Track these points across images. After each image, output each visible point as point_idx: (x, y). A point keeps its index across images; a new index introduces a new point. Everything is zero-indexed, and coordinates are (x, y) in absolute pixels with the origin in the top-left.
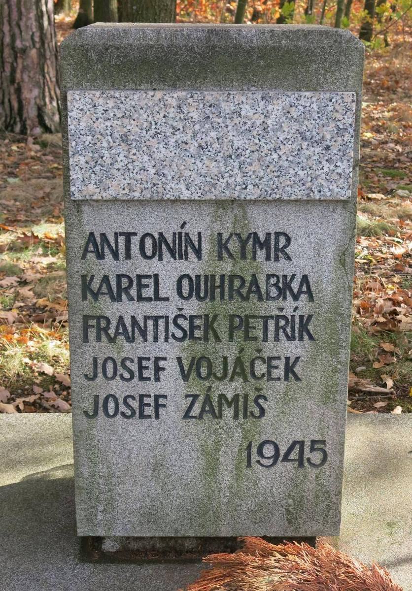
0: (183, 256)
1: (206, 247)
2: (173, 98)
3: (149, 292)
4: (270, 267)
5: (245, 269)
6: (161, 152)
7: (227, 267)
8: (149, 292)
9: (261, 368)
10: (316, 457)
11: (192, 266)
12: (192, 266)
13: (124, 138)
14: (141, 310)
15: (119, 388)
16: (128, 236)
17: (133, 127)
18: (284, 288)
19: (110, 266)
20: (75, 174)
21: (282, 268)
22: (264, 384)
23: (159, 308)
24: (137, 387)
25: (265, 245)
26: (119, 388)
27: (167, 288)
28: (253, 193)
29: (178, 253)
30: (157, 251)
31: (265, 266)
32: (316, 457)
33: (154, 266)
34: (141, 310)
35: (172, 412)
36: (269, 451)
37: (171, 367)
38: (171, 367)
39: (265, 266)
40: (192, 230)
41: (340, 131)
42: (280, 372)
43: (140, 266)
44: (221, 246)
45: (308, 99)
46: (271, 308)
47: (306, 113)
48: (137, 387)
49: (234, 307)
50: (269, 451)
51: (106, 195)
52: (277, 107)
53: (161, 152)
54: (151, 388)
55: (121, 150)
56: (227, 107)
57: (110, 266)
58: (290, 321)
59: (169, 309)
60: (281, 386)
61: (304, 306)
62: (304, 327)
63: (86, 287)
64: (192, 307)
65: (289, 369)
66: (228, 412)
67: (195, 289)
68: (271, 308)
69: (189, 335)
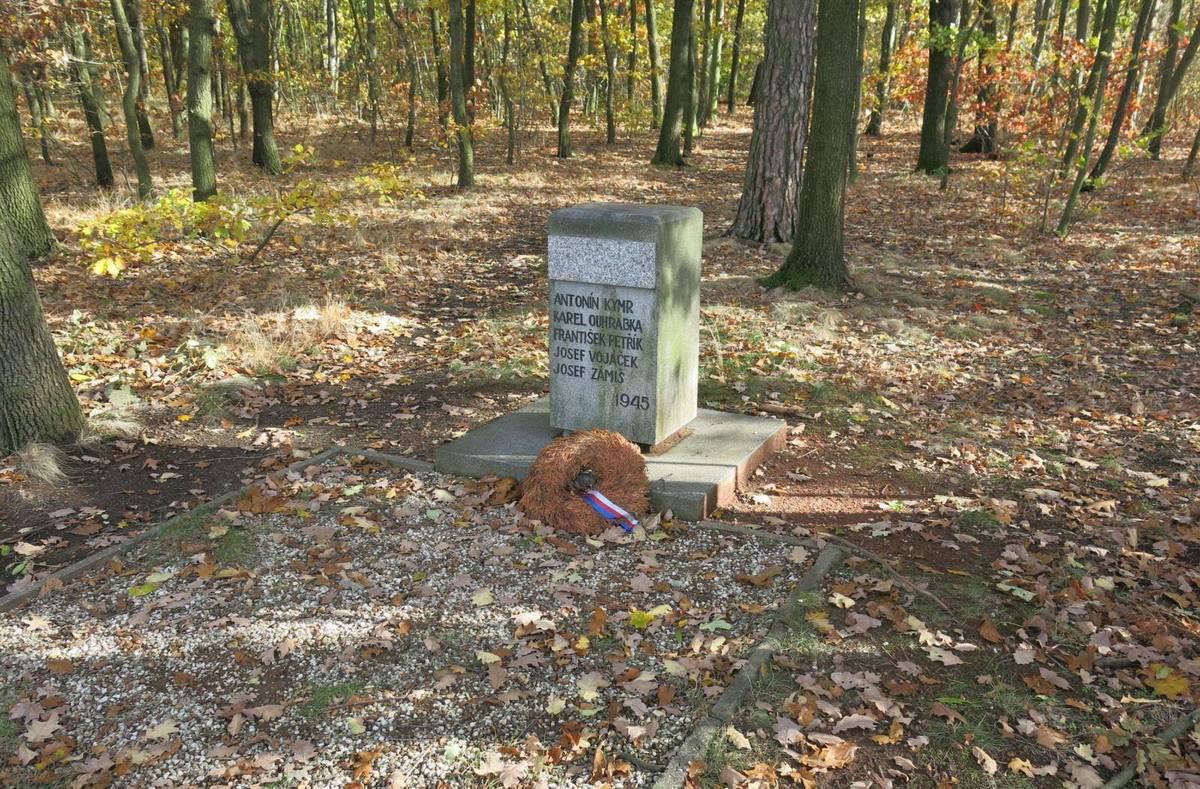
0: (592, 307)
1: (600, 304)
2: (585, 240)
3: (578, 321)
4: (624, 315)
6: (581, 262)
8: (578, 321)
9: (622, 360)
10: (644, 405)
11: (595, 312)
12: (595, 312)
13: (568, 256)
14: (576, 328)
15: (567, 362)
16: (571, 296)
17: (570, 251)
18: (631, 326)
19: (564, 308)
21: (629, 316)
24: (574, 362)
26: (567, 362)
27: (586, 320)
28: (614, 283)
30: (582, 305)
34: (576, 328)
35: (587, 375)
37: (586, 355)
38: (586, 354)
40: (595, 296)
41: (648, 259)
42: (629, 363)
43: (575, 309)
44: (606, 304)
45: (636, 245)
46: (625, 333)
47: (635, 251)
48: (574, 362)
49: (611, 331)
51: (562, 278)
52: (623, 248)
53: (581, 262)
54: (579, 363)
56: (605, 246)
57: (564, 308)
58: (633, 340)
59: (586, 329)
60: (630, 369)
62: (638, 344)
64: (595, 330)
65: (633, 362)
66: (609, 379)
67: (596, 322)
68: (625, 333)
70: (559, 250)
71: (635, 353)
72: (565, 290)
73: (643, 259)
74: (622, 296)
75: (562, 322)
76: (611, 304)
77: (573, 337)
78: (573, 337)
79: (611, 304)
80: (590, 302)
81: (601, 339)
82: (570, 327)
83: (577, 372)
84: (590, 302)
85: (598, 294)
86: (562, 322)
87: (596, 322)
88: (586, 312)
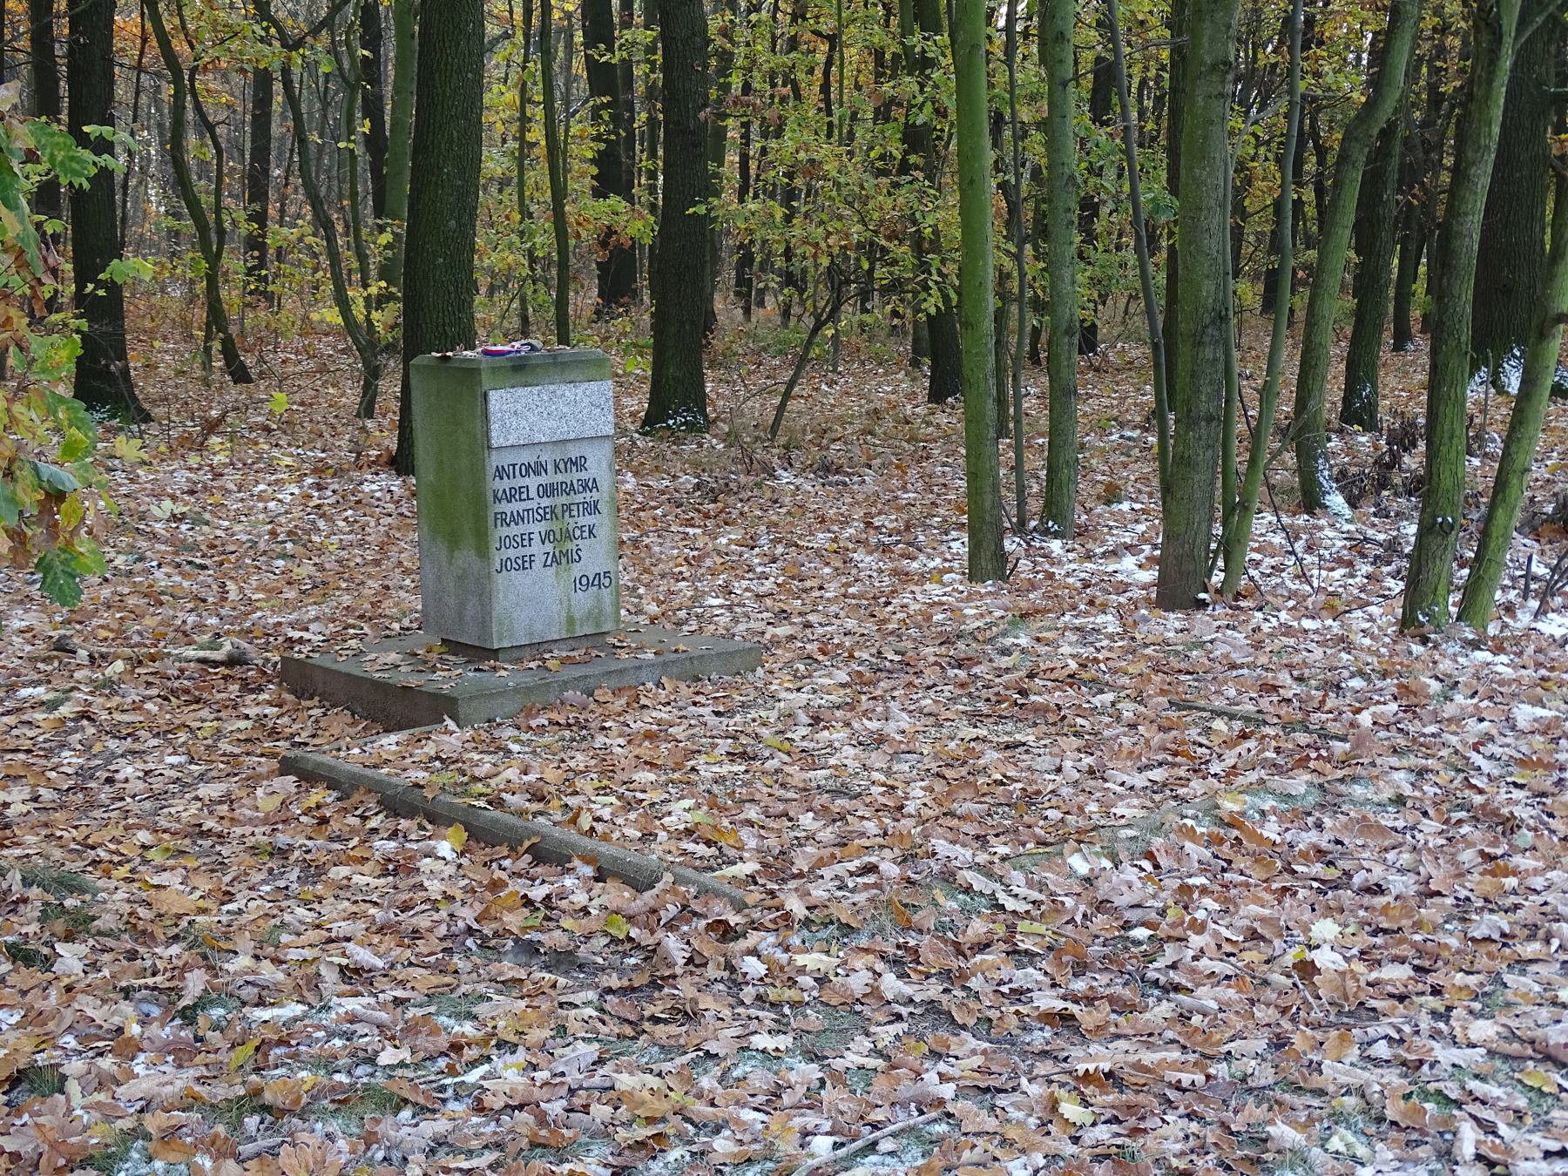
1: (550, 468)
2: (535, 390)
3: (524, 496)
7: (560, 478)
8: (524, 496)
9: (578, 533)
11: (543, 479)
12: (543, 479)
14: (524, 505)
15: (512, 553)
17: (519, 407)
18: (585, 487)
20: (494, 434)
21: (583, 475)
22: (579, 542)
24: (521, 551)
25: (575, 464)
26: (512, 553)
27: (533, 493)
29: (537, 473)
31: (574, 476)
33: (527, 481)
35: (538, 564)
39: (574, 476)
40: (542, 459)
42: (586, 534)
43: (519, 482)
46: (579, 498)
48: (521, 551)
49: (564, 499)
52: (580, 391)
54: (527, 551)
55: (514, 419)
59: (532, 505)
61: (595, 495)
64: (545, 502)
68: (579, 498)
70: (505, 407)
71: (587, 520)
72: (505, 460)
73: (602, 401)
74: (574, 452)
75: (504, 502)
76: (562, 466)
77: (518, 518)
79: (562, 466)
80: (537, 469)
81: (553, 512)
82: (516, 506)
84: (537, 469)
86: (504, 502)
87: (545, 491)
88: (533, 482)
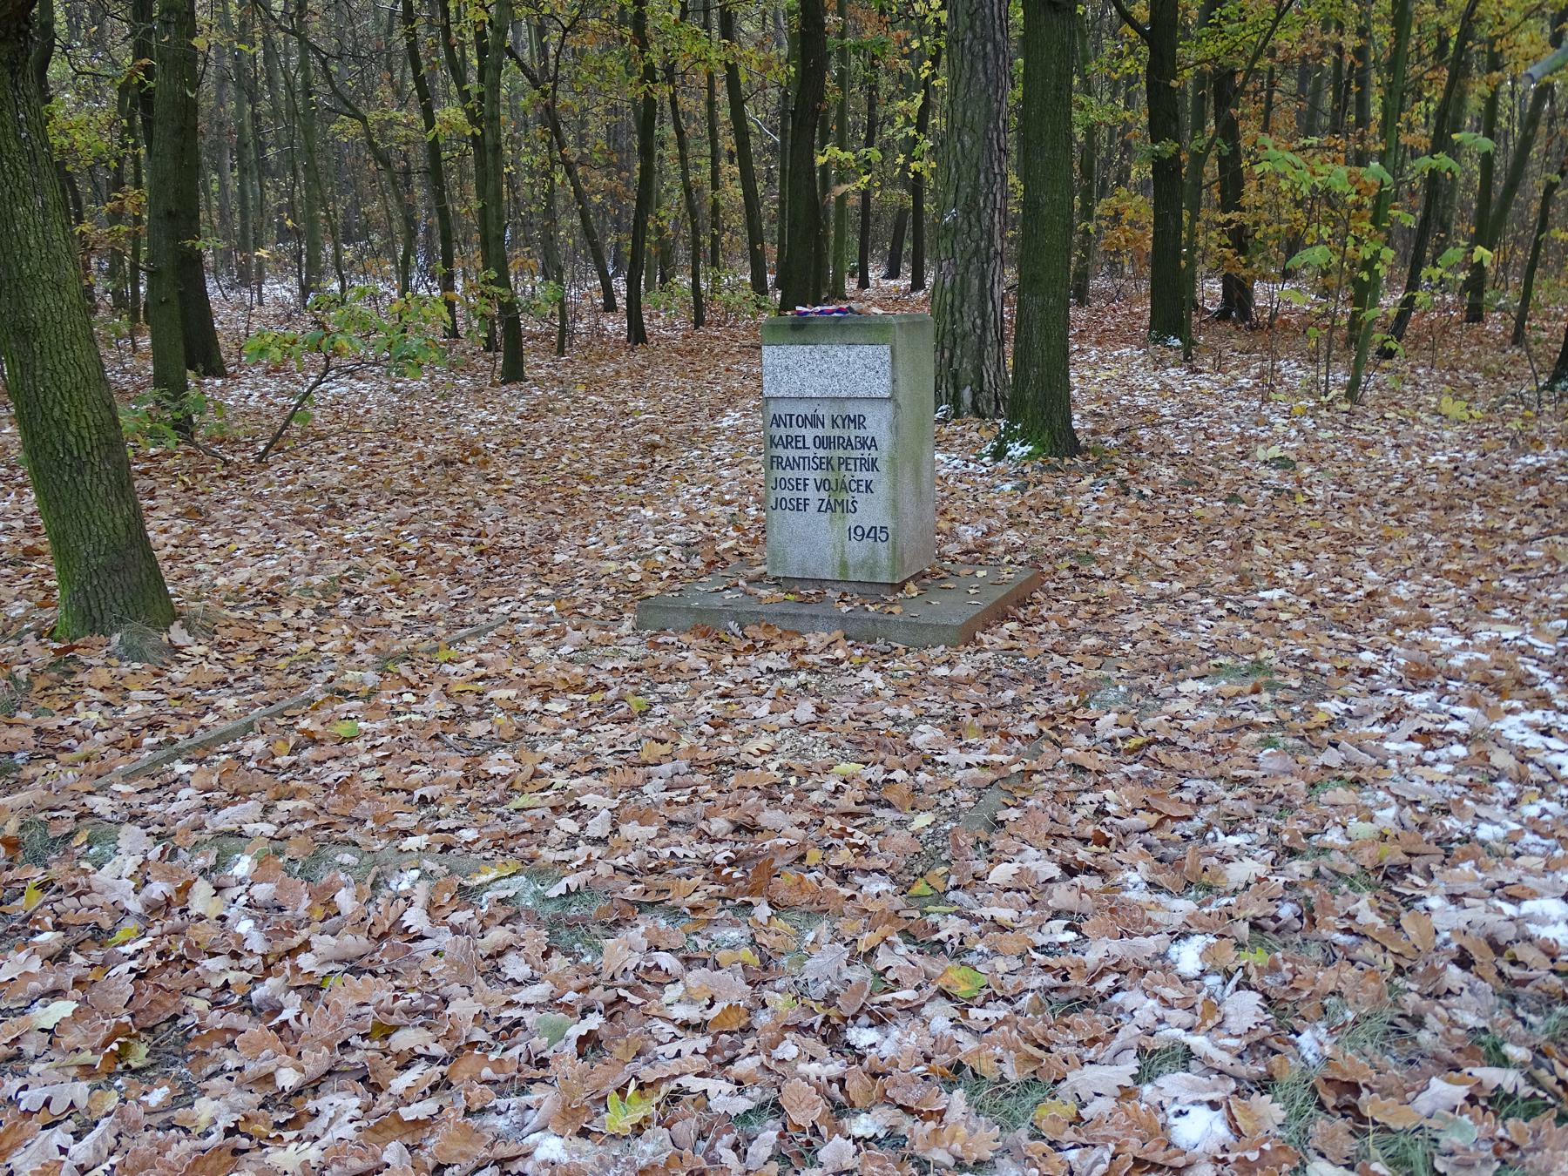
1: (827, 422)
5: (845, 433)
9: (854, 486)
10: (883, 537)
11: (820, 432)
12: (820, 432)
14: (797, 453)
15: (786, 494)
19: (782, 431)
21: (862, 433)
23: (805, 453)
26: (786, 494)
27: (809, 443)
31: (852, 433)
32: (883, 537)
33: (803, 431)
34: (797, 453)
35: (813, 506)
36: (859, 531)
38: (811, 483)
39: (852, 433)
40: (820, 413)
42: (863, 488)
44: (834, 421)
46: (857, 454)
49: (841, 453)
50: (859, 531)
54: (802, 495)
57: (782, 431)
60: (864, 495)
63: (772, 441)
64: (821, 453)
65: (868, 487)
66: (839, 509)
68: (857, 454)
69: (819, 467)
71: (865, 475)
72: (783, 409)
74: (853, 410)
76: (839, 421)
77: (793, 464)
78: (793, 464)
79: (839, 421)
80: (815, 421)
82: (791, 453)
83: (800, 505)
84: (815, 421)
85: (824, 411)
87: (822, 443)
88: (809, 433)
